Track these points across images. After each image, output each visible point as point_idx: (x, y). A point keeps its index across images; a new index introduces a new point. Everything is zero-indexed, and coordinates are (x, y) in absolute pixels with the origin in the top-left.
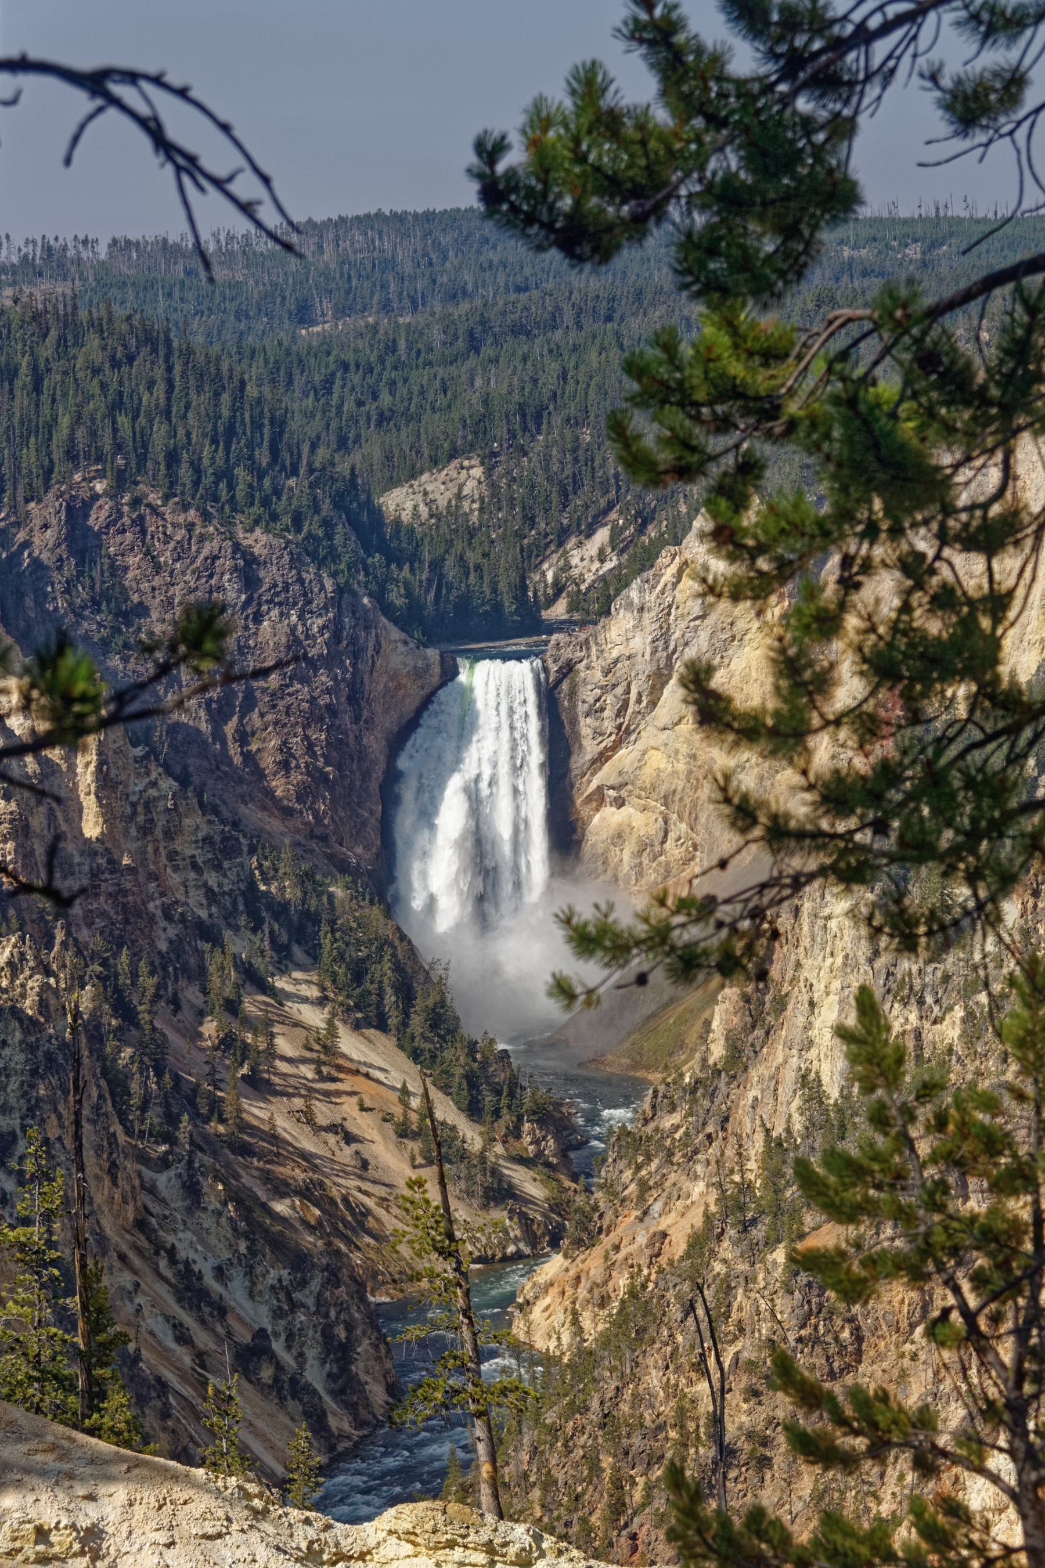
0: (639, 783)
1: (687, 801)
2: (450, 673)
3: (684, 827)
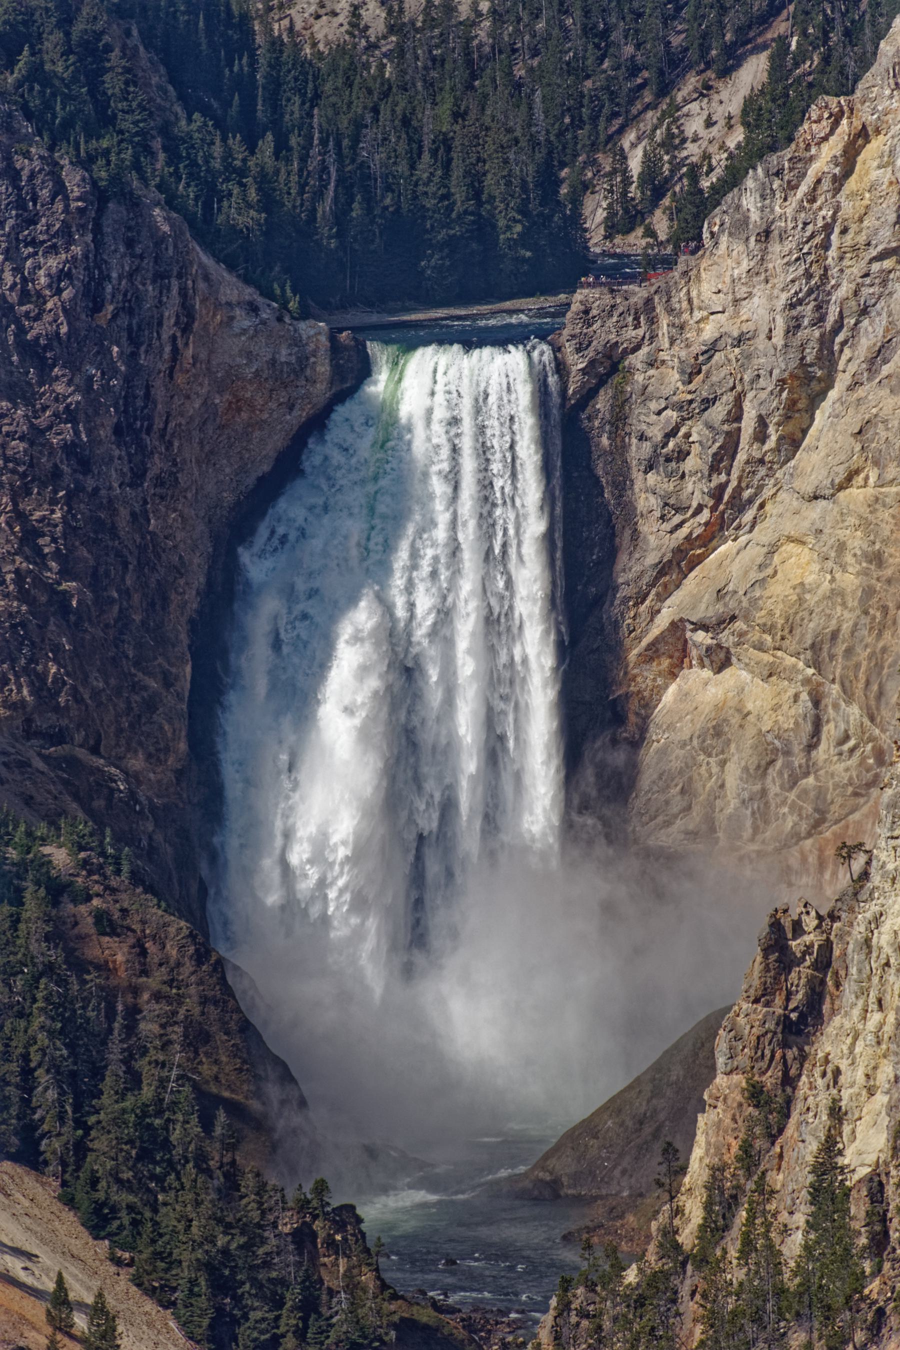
0: (760, 616)
1: (863, 655)
2: (354, 372)
3: (854, 712)
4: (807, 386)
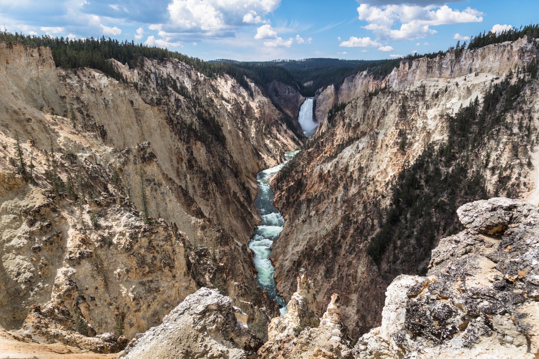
4: (323, 101)
